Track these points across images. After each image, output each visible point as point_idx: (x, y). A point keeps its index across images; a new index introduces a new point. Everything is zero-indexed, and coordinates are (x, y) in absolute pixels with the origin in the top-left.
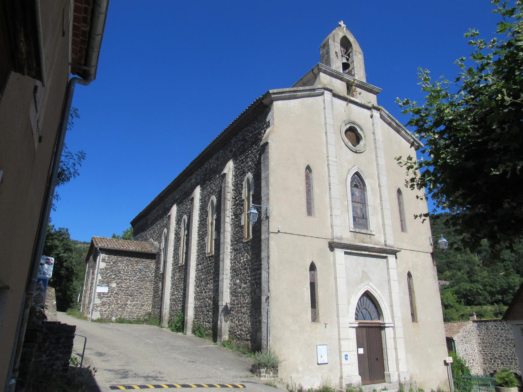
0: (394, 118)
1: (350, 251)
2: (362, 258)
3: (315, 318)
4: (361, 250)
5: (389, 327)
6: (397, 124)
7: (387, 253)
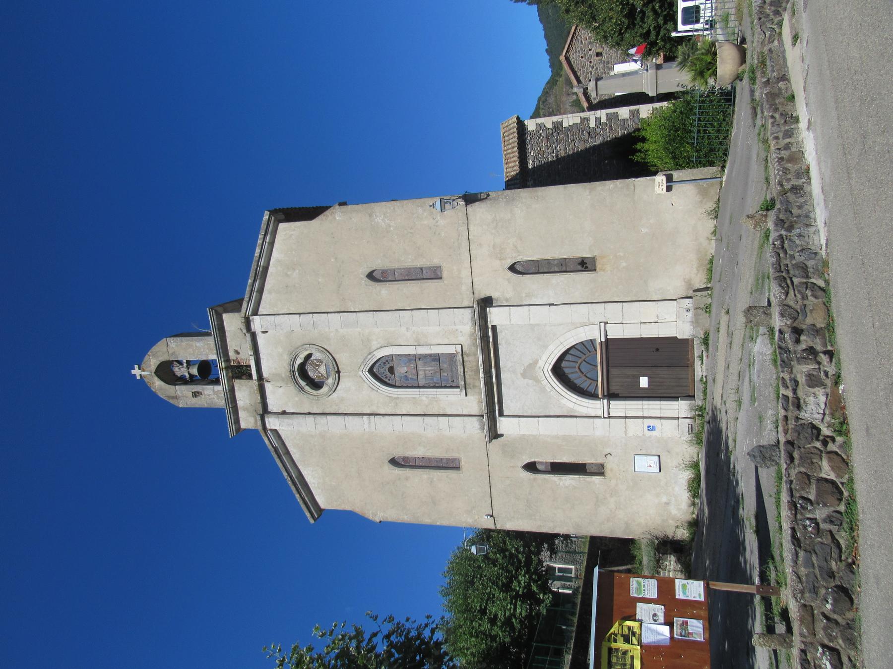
0: (248, 289)
1: (493, 370)
2: (503, 377)
3: (599, 471)
4: (488, 342)
5: (606, 332)
6: (255, 281)
7: (487, 327)
